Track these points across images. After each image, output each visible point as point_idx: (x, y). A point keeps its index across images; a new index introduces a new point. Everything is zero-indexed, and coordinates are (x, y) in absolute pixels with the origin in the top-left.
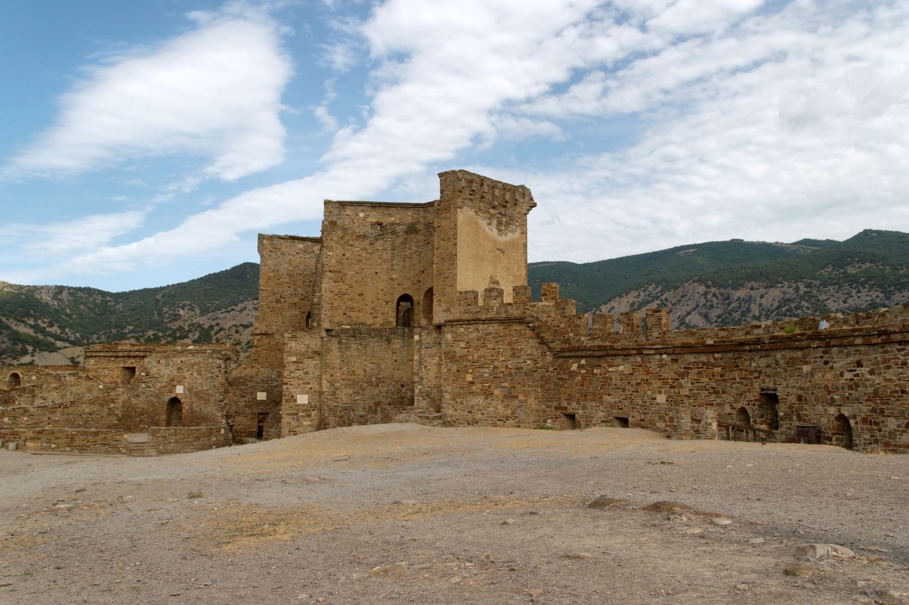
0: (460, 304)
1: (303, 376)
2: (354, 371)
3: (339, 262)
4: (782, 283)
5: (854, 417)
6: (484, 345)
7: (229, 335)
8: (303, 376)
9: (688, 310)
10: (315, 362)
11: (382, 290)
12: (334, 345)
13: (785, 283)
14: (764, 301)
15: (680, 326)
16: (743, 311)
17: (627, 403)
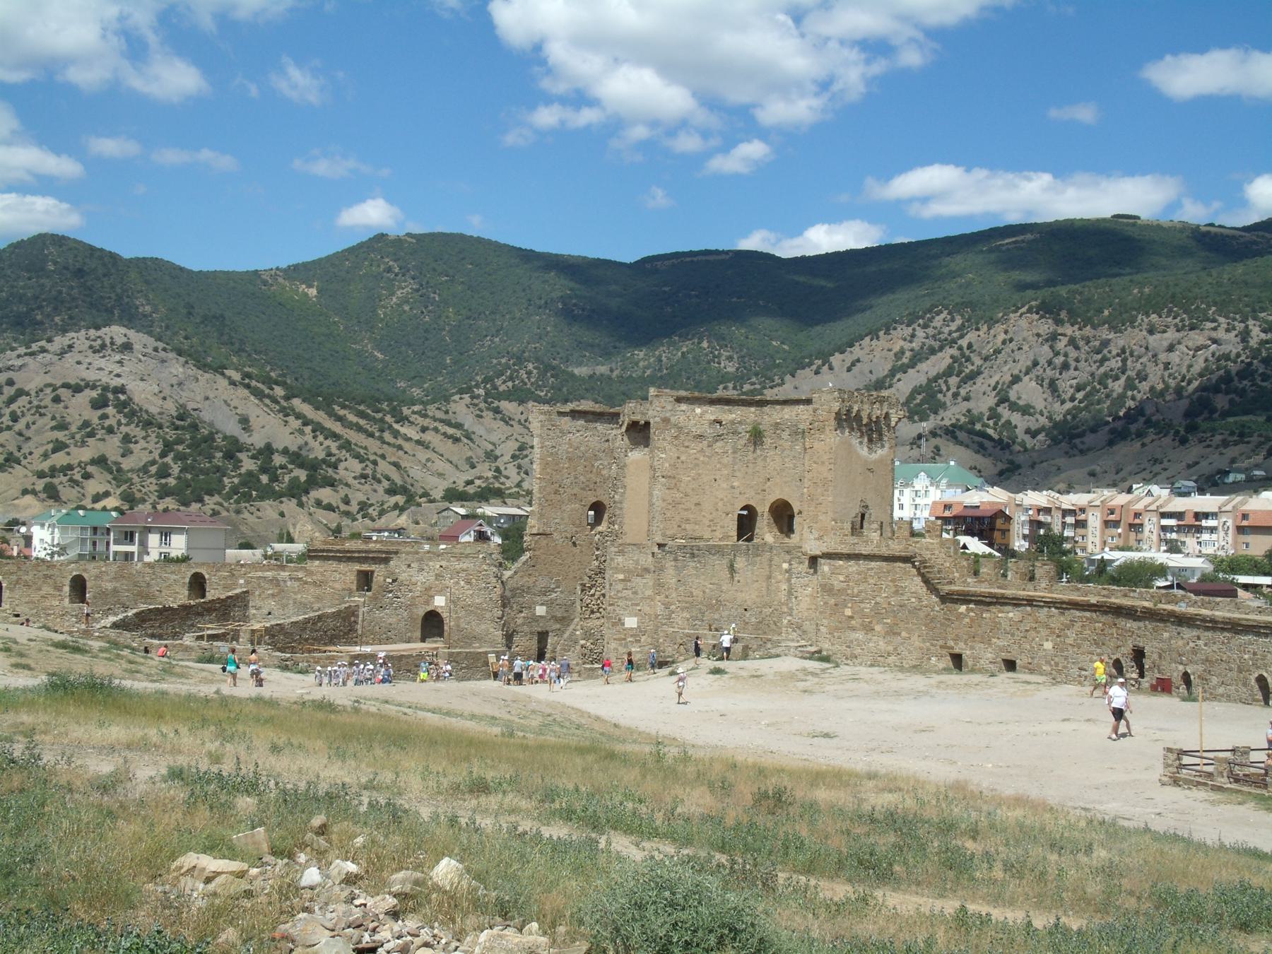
0: (835, 534)
1: (632, 596)
2: (691, 593)
3: (674, 466)
4: (1214, 321)
5: (1194, 674)
6: (865, 580)
7: (39, 407)
8: (632, 596)
9: (1016, 372)
10: (645, 581)
11: (722, 500)
12: (669, 564)
13: (1222, 320)
14: (1174, 357)
15: (997, 405)
16: (1128, 378)
17: (1016, 647)
